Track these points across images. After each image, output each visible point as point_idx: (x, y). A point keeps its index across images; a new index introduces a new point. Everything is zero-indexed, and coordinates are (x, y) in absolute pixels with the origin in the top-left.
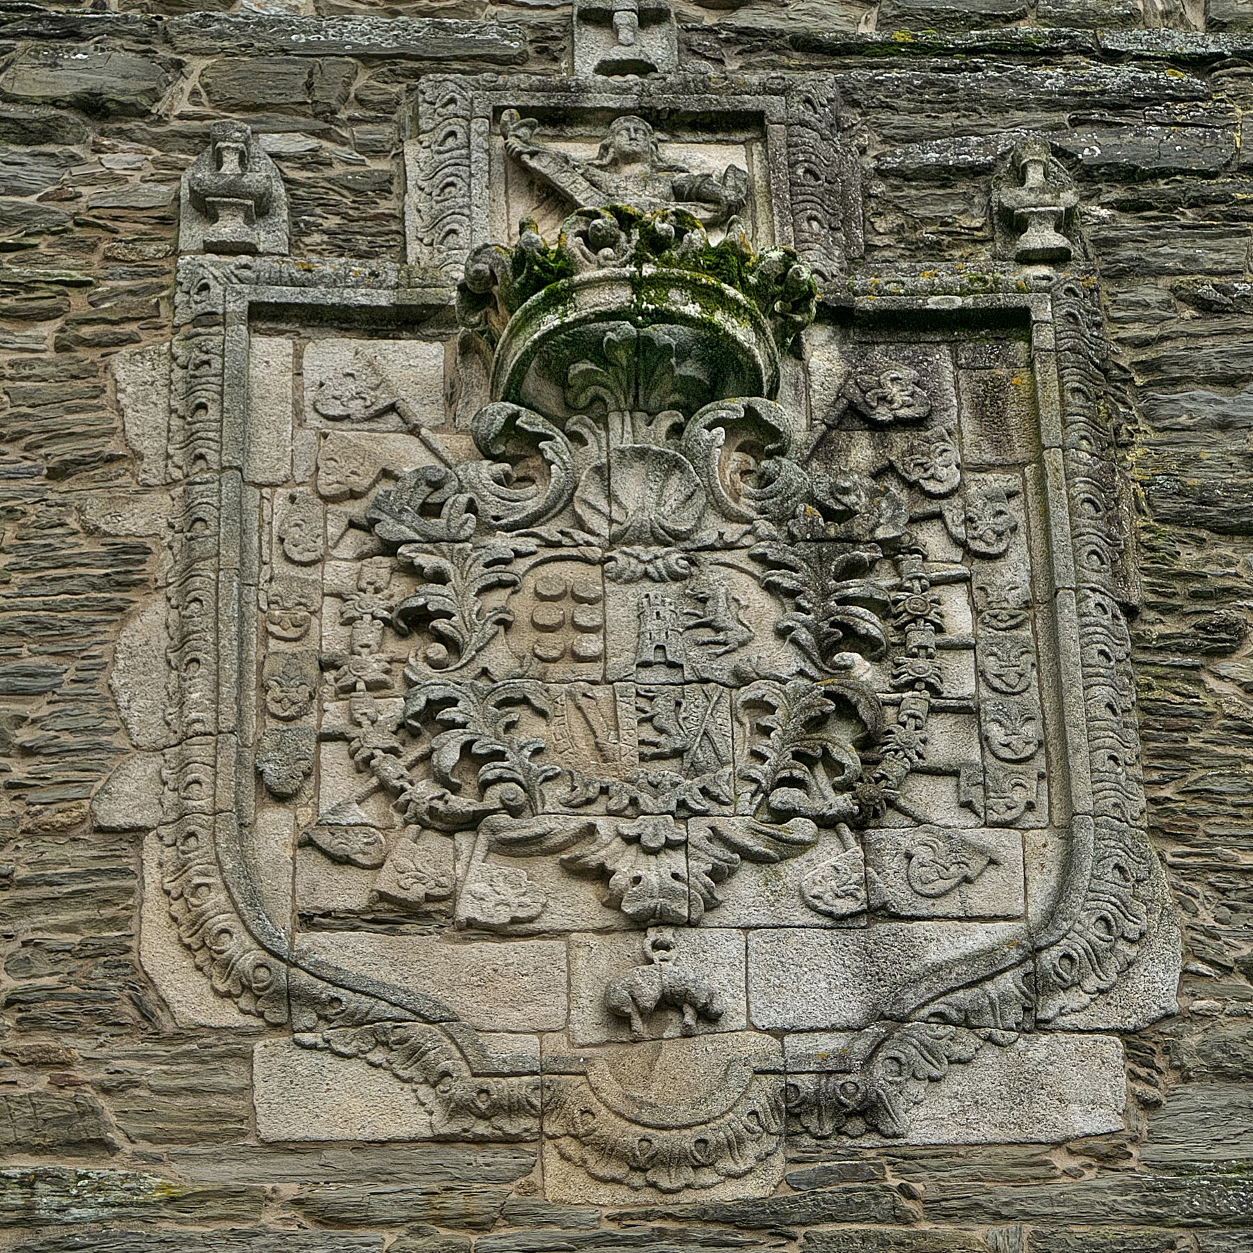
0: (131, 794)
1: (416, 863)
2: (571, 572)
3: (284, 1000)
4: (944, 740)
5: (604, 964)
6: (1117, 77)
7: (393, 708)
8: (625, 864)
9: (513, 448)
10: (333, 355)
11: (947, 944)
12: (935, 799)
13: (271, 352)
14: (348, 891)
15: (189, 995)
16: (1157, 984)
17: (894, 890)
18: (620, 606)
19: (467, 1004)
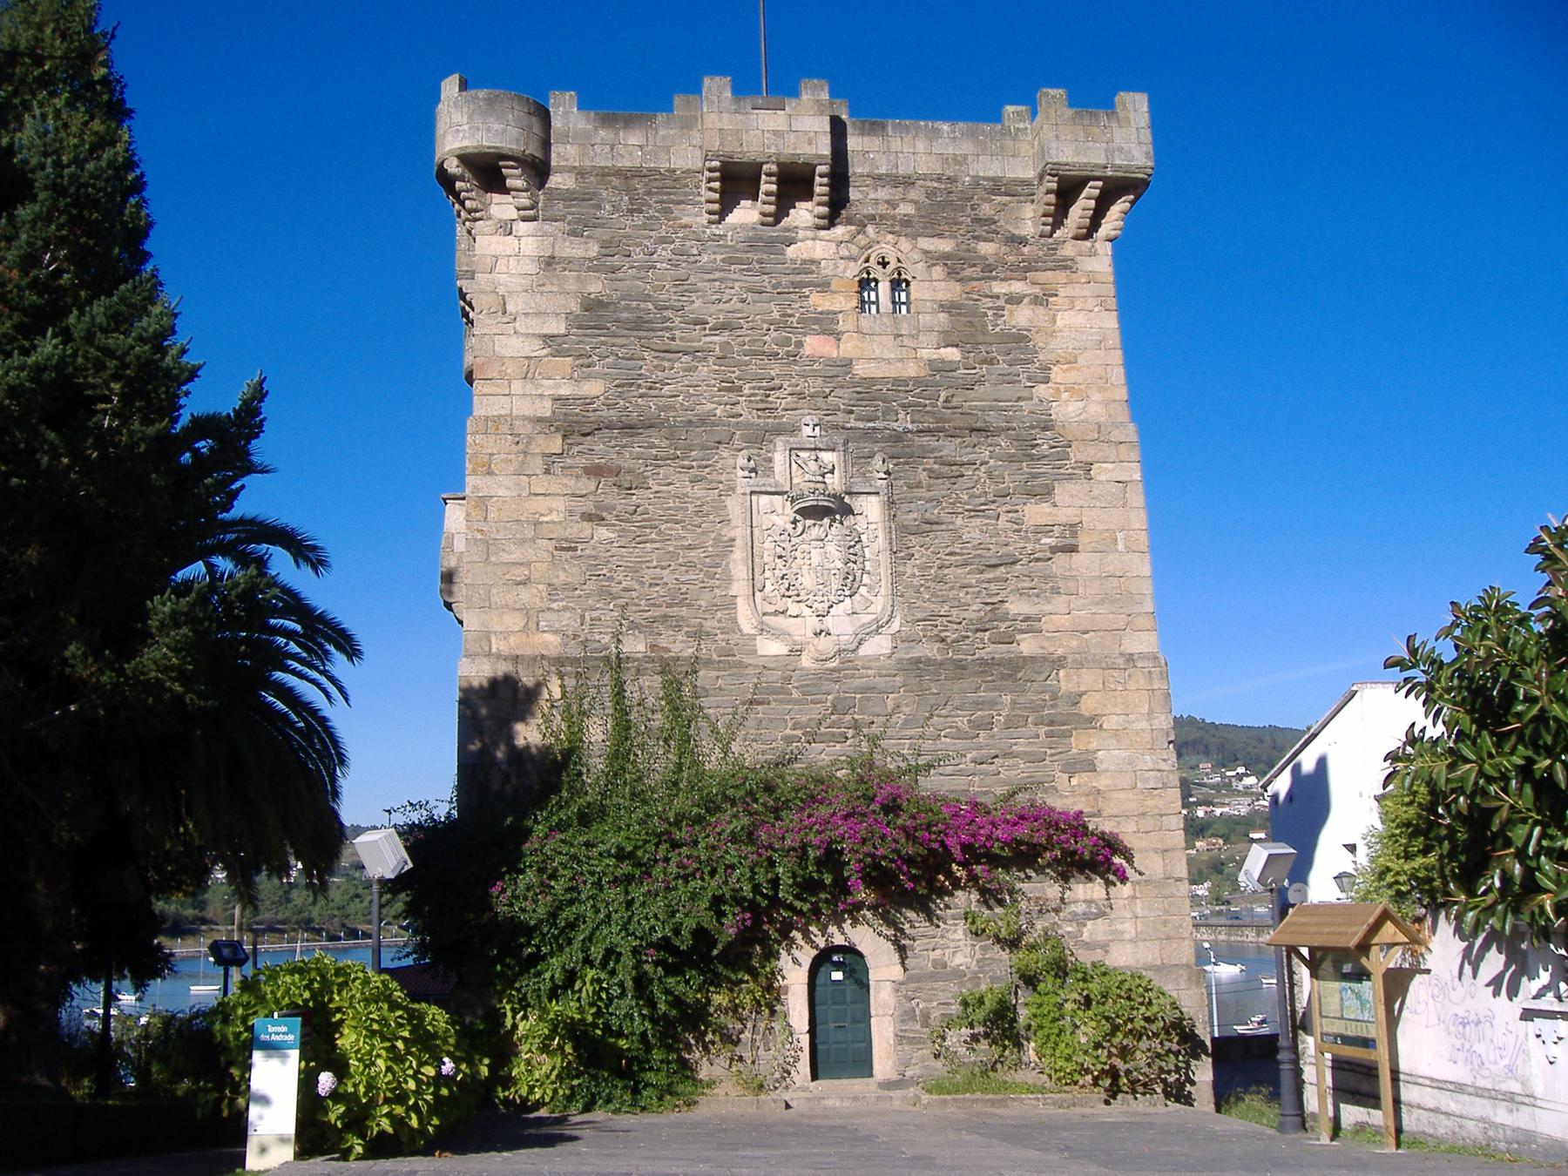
2: (805, 547)
9: (795, 522)
10: (764, 499)
12: (863, 590)
14: (771, 609)
19: (790, 631)
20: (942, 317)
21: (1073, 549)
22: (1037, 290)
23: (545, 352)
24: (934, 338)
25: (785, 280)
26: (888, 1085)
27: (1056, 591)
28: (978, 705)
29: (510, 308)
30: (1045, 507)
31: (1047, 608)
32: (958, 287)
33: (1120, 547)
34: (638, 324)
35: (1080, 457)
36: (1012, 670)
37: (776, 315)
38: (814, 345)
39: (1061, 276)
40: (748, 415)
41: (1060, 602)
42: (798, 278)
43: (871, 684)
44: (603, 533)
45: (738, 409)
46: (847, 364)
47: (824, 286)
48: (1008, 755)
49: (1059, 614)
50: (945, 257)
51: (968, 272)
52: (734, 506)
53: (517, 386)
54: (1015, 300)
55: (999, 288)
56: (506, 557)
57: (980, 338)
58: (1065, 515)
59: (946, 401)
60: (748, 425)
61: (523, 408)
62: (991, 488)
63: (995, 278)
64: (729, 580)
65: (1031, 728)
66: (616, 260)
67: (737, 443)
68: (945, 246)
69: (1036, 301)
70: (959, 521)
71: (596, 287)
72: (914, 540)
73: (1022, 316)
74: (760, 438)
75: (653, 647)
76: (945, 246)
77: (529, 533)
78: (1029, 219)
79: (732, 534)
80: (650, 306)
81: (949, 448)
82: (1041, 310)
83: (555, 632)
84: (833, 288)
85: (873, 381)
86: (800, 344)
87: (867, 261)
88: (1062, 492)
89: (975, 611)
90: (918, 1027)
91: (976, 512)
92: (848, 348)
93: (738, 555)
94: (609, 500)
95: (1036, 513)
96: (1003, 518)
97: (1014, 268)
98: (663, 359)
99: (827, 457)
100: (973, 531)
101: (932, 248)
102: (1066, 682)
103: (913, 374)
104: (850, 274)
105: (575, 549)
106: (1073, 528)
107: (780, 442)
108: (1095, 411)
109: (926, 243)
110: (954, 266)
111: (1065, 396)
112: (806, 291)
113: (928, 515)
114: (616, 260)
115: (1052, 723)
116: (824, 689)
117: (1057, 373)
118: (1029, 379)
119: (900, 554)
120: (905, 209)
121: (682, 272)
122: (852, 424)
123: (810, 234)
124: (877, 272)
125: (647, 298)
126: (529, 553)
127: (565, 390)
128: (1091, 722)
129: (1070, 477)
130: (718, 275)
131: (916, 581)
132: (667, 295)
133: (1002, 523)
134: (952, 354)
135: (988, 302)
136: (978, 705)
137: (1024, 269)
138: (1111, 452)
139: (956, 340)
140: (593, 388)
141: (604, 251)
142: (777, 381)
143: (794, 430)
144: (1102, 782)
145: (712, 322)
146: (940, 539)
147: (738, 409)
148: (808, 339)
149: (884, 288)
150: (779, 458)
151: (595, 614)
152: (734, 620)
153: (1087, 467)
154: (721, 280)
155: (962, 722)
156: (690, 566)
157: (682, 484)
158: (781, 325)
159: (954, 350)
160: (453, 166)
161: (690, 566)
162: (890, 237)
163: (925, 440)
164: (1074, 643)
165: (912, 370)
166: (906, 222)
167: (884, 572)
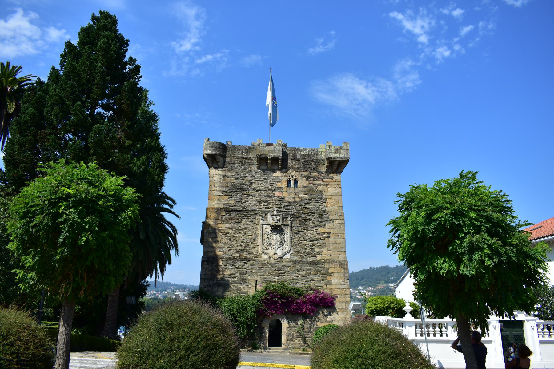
10: (265, 226)
11: (285, 251)
15: (260, 252)
20: (304, 188)
21: (329, 237)
24: (302, 193)
26: (284, 349)
27: (325, 246)
28: (308, 270)
30: (323, 229)
31: (323, 250)
34: (242, 189)
36: (315, 264)
38: (277, 194)
39: (330, 180)
40: (263, 209)
41: (326, 249)
44: (232, 232)
47: (280, 182)
48: (313, 280)
49: (325, 251)
50: (305, 176)
51: (310, 179)
52: (259, 227)
53: (216, 201)
54: (320, 185)
55: (317, 182)
58: (327, 230)
60: (263, 211)
61: (217, 206)
62: (313, 225)
64: (257, 242)
65: (318, 275)
66: (238, 176)
67: (260, 214)
69: (324, 185)
71: (234, 181)
72: (296, 235)
73: (320, 188)
78: (324, 169)
81: (304, 216)
82: (325, 187)
85: (288, 202)
86: (274, 194)
88: (327, 226)
89: (308, 250)
91: (309, 230)
92: (285, 194)
93: (259, 237)
94: (234, 225)
95: (321, 230)
97: (320, 178)
99: (278, 217)
100: (308, 233)
102: (326, 266)
106: (329, 233)
107: (269, 214)
108: (336, 208)
109: (301, 173)
110: (307, 178)
114: (238, 176)
119: (292, 238)
120: (298, 166)
121: (251, 178)
122: (284, 210)
124: (292, 179)
125: (243, 184)
127: (226, 202)
129: (329, 223)
132: (248, 183)
134: (306, 196)
135: (314, 186)
136: (308, 270)
137: (322, 179)
140: (232, 202)
143: (272, 212)
144: (333, 287)
145: (257, 189)
146: (301, 235)
149: (292, 182)
150: (269, 217)
153: (333, 220)
155: (304, 273)
156: (249, 239)
157: (249, 222)
158: (270, 190)
160: (206, 156)
161: (249, 239)
164: (328, 258)
165: (297, 199)
166: (298, 168)
167: (289, 241)
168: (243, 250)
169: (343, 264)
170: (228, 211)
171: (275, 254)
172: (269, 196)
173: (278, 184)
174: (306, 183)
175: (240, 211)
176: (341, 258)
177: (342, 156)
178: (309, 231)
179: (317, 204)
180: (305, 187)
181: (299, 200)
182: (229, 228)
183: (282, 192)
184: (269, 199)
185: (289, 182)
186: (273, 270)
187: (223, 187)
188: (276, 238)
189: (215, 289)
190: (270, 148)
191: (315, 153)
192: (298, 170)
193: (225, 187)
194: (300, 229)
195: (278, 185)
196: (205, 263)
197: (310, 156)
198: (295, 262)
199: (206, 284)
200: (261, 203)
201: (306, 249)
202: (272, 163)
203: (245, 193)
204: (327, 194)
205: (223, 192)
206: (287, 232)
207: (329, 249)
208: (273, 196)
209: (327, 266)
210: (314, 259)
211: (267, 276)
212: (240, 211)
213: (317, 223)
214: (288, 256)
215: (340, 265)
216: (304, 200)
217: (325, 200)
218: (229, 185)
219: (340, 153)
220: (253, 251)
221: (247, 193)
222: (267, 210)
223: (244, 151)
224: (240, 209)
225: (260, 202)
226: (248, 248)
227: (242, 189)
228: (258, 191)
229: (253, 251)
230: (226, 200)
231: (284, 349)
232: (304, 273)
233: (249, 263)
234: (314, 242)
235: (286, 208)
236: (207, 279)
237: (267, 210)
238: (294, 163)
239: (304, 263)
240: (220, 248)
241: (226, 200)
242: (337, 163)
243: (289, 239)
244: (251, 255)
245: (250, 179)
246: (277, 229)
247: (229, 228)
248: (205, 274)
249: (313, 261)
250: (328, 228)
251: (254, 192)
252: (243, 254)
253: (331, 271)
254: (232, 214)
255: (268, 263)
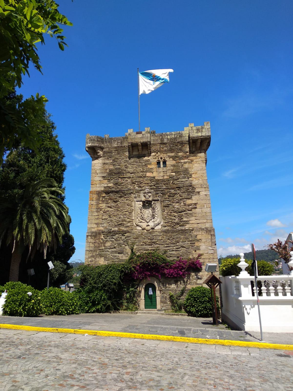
0: (133, 218)
1: (141, 220)
3: (137, 225)
4: (156, 215)
5: (146, 224)
6: (162, 189)
7: (141, 215)
8: (147, 221)
10: (139, 202)
11: (156, 222)
12: (156, 217)
13: (137, 202)
14: (140, 221)
16: (162, 223)
17: (155, 221)
18: (147, 211)
21: (196, 208)
22: (190, 161)
23: (103, 179)
24: (170, 171)
25: (144, 163)
26: (159, 310)
29: (97, 172)
31: (191, 219)
32: (175, 162)
33: (205, 207)
34: (119, 173)
35: (197, 191)
36: (184, 232)
37: (142, 170)
38: (148, 174)
40: (137, 188)
41: (193, 218)
42: (145, 163)
43: (157, 234)
44: (111, 209)
45: (135, 187)
46: (154, 177)
47: (150, 164)
49: (193, 220)
51: (177, 159)
54: (185, 163)
55: (182, 161)
56: (95, 215)
57: (179, 171)
58: (194, 202)
59: (172, 182)
61: (98, 189)
63: (182, 159)
68: (173, 154)
69: (189, 163)
70: (174, 204)
71: (112, 167)
72: (165, 208)
73: (186, 166)
74: (138, 192)
75: (119, 229)
76: (173, 154)
77: (99, 210)
79: (133, 209)
80: (120, 170)
81: (172, 191)
82: (190, 164)
83: (103, 227)
84: (152, 164)
85: (158, 180)
86: (146, 175)
87: (158, 158)
88: (194, 198)
90: (164, 300)
91: (177, 203)
92: (155, 174)
95: (189, 202)
96: (182, 203)
97: (185, 157)
98: (122, 179)
100: (177, 206)
101: (170, 155)
103: (166, 178)
104: (155, 161)
105: (106, 213)
106: (196, 204)
108: (201, 182)
109: (168, 154)
110: (174, 158)
111: (195, 180)
112: (147, 165)
113: (168, 203)
114: (115, 163)
115: (191, 241)
116: (148, 235)
117: (193, 176)
118: (188, 177)
119: (163, 211)
121: (126, 164)
122: (155, 188)
123: (148, 155)
125: (119, 169)
126: (99, 214)
127: (106, 186)
128: (198, 241)
129: (196, 195)
130: (133, 164)
131: (166, 215)
133: (182, 204)
134: (174, 174)
137: (187, 157)
138: (204, 189)
139: (174, 171)
140: (110, 185)
141: (113, 161)
142: (142, 182)
145: (131, 172)
147: (135, 187)
148: (147, 173)
149: (161, 163)
151: (109, 224)
152: (133, 224)
153: (199, 193)
154: (133, 164)
159: (174, 173)
161: (125, 214)
162: (162, 154)
163: (168, 190)
165: (166, 177)
168: (121, 224)
169: (210, 231)
170: (107, 193)
171: (148, 225)
172: (141, 177)
173: (149, 166)
174: (174, 162)
175: (117, 192)
176: (208, 225)
177: (204, 134)
178: (177, 204)
179: (184, 180)
180: (172, 166)
181: (168, 177)
182: (109, 207)
183: (152, 172)
184: (141, 179)
185: (158, 163)
186: (146, 240)
187: (102, 173)
188: (148, 212)
189: (98, 259)
190: (140, 136)
191: (180, 136)
192: (166, 152)
193: (105, 173)
194: (169, 203)
195: (149, 166)
196: (89, 237)
197: (175, 138)
198: (166, 232)
199: (90, 255)
200: (135, 184)
201: (175, 220)
202: (142, 148)
203: (121, 176)
204: (193, 170)
205: (103, 177)
206: (158, 207)
207: (197, 218)
208: (145, 177)
209: (195, 234)
210: (183, 228)
211: (141, 245)
212: (117, 192)
213: (185, 195)
214: (159, 227)
215: (207, 232)
216: (171, 177)
217: (191, 175)
218: (108, 171)
219: (202, 131)
220: (129, 224)
221: (123, 176)
222: (140, 189)
223: (119, 141)
224: (117, 190)
225: (133, 183)
226: (124, 223)
227: (119, 173)
228: (131, 173)
229: (129, 224)
230: (106, 183)
231: (159, 310)
232: (174, 241)
233: (126, 235)
234: (183, 213)
235: (156, 185)
236: (91, 251)
237: (140, 189)
238: (162, 146)
239: (173, 232)
240: (101, 224)
241: (106, 183)
242: (199, 141)
243: (160, 211)
244: (127, 228)
245: (125, 164)
246: (147, 204)
247: (109, 207)
248: (89, 247)
249: (182, 230)
250: (195, 199)
251: (129, 175)
252: (121, 228)
253: (199, 237)
254: (111, 194)
255: (142, 234)
